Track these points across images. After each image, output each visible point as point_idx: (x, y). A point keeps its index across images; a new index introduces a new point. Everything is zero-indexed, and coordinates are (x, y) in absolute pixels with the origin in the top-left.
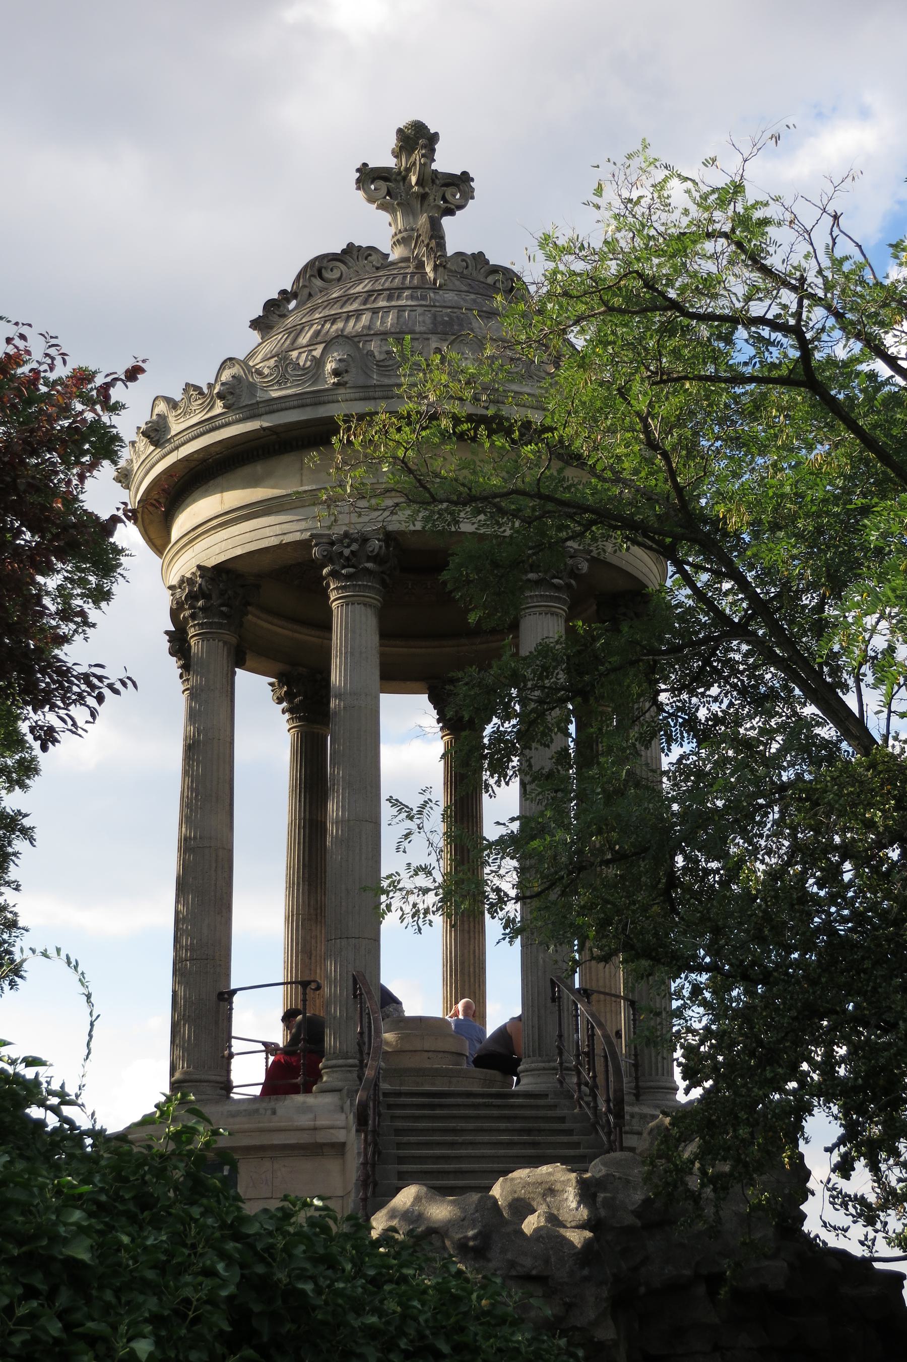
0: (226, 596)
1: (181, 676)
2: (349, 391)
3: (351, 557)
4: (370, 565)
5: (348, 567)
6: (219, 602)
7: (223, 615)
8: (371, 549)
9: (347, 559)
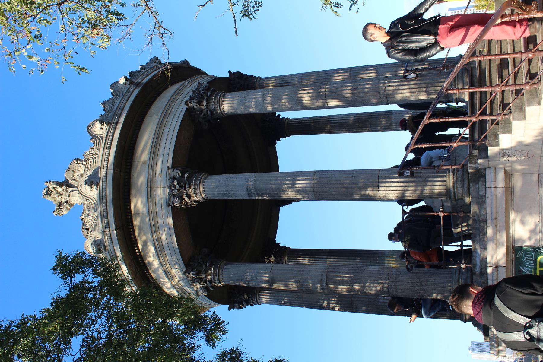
1: (252, 305)
4: (186, 176)
7: (211, 265)
8: (177, 174)
9: (181, 187)
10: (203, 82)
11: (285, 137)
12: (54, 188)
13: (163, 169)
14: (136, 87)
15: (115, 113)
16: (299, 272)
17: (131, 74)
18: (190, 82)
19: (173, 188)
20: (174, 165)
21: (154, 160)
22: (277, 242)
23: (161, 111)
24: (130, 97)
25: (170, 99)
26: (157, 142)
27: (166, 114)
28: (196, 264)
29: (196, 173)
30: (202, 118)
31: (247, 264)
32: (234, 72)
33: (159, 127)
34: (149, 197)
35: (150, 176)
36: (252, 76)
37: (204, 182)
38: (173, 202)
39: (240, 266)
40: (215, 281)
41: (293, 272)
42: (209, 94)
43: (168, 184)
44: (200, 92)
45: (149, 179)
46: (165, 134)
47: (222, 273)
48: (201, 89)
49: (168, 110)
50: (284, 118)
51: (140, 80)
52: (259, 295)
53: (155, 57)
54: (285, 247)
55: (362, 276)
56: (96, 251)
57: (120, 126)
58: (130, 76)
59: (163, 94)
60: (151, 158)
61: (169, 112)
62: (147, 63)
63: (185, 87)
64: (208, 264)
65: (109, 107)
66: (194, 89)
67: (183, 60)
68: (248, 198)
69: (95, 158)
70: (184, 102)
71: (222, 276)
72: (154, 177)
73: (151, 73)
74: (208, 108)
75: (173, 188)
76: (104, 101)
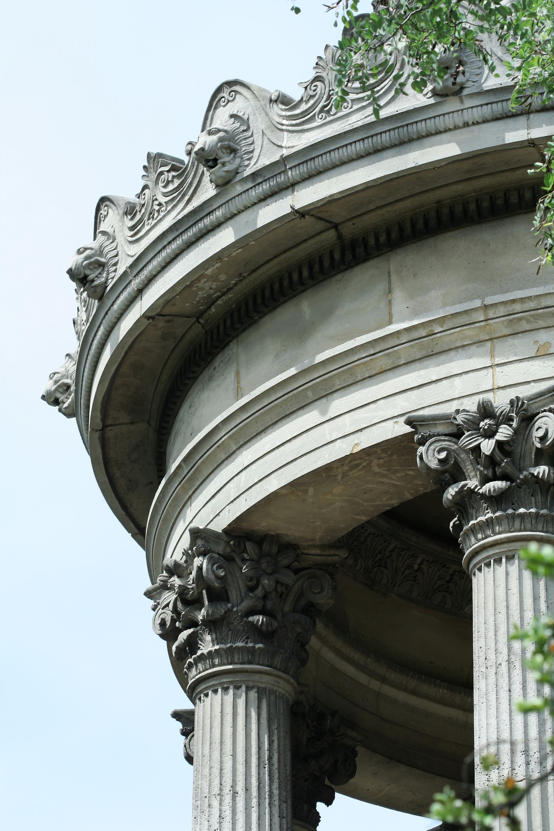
0: (259, 592)
2: (468, 103)
3: (498, 456)
5: (495, 478)
6: (246, 605)
8: (541, 433)
9: (491, 461)
19: (484, 424)
34: (449, 324)
45: (518, 307)
56: (202, 149)
72: (535, 326)
75: (484, 424)
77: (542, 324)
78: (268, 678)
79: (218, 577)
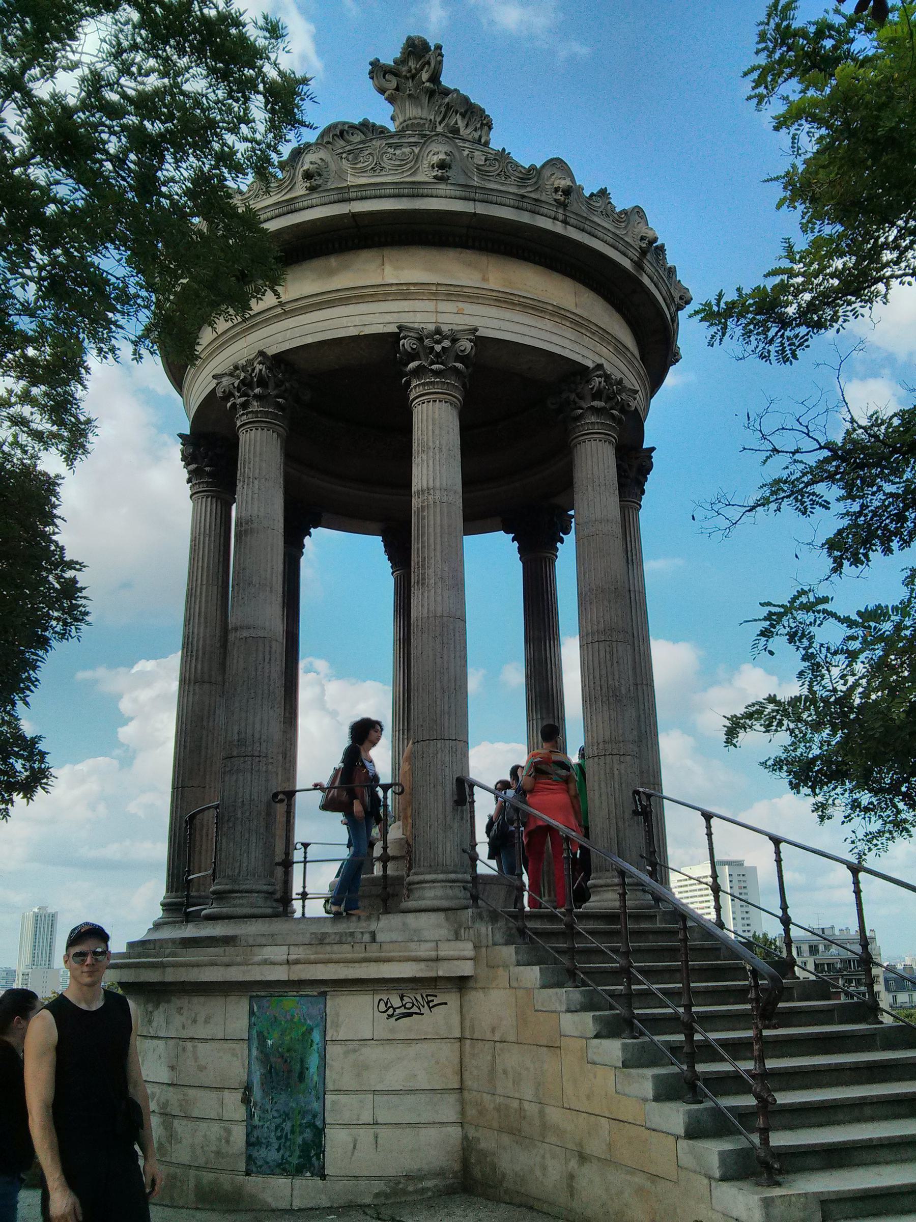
0: (283, 388)
1: (189, 481)
2: (449, 187)
5: (438, 363)
7: (279, 406)
8: (462, 348)
9: (438, 355)
10: (638, 398)
11: (520, 550)
12: (429, 63)
13: (472, 318)
14: (634, 262)
15: (586, 219)
16: (268, 584)
17: (661, 248)
18: (639, 373)
20: (481, 342)
21: (489, 299)
22: (312, 530)
23: (585, 315)
24: (617, 249)
25: (608, 333)
26: (525, 306)
27: (579, 323)
28: (280, 376)
29: (464, 386)
30: (568, 397)
31: (281, 480)
32: (652, 457)
33: (555, 310)
35: (459, 289)
36: (643, 492)
37: (446, 402)
38: (409, 336)
39: (279, 466)
40: (247, 414)
41: (269, 571)
42: (614, 412)
43: (445, 329)
44: (619, 394)
45: (452, 288)
46: (540, 323)
47: (262, 429)
48: (624, 396)
49: (587, 328)
50: (557, 549)
51: (648, 271)
52: (212, 497)
53: (692, 299)
54: (303, 546)
55: (262, 705)
57: (558, 228)
58: (657, 247)
59: (617, 316)
60: (494, 294)
61: (583, 331)
62: (679, 281)
63: (631, 363)
64: (280, 400)
65: (598, 205)
66: (625, 382)
67: (682, 352)
68: (414, 489)
69: (498, 175)
70: (599, 362)
71: (257, 429)
73: (661, 293)
74: (586, 411)
76: (609, 194)
77: (461, 299)
78: (281, 429)
79: (268, 376)
